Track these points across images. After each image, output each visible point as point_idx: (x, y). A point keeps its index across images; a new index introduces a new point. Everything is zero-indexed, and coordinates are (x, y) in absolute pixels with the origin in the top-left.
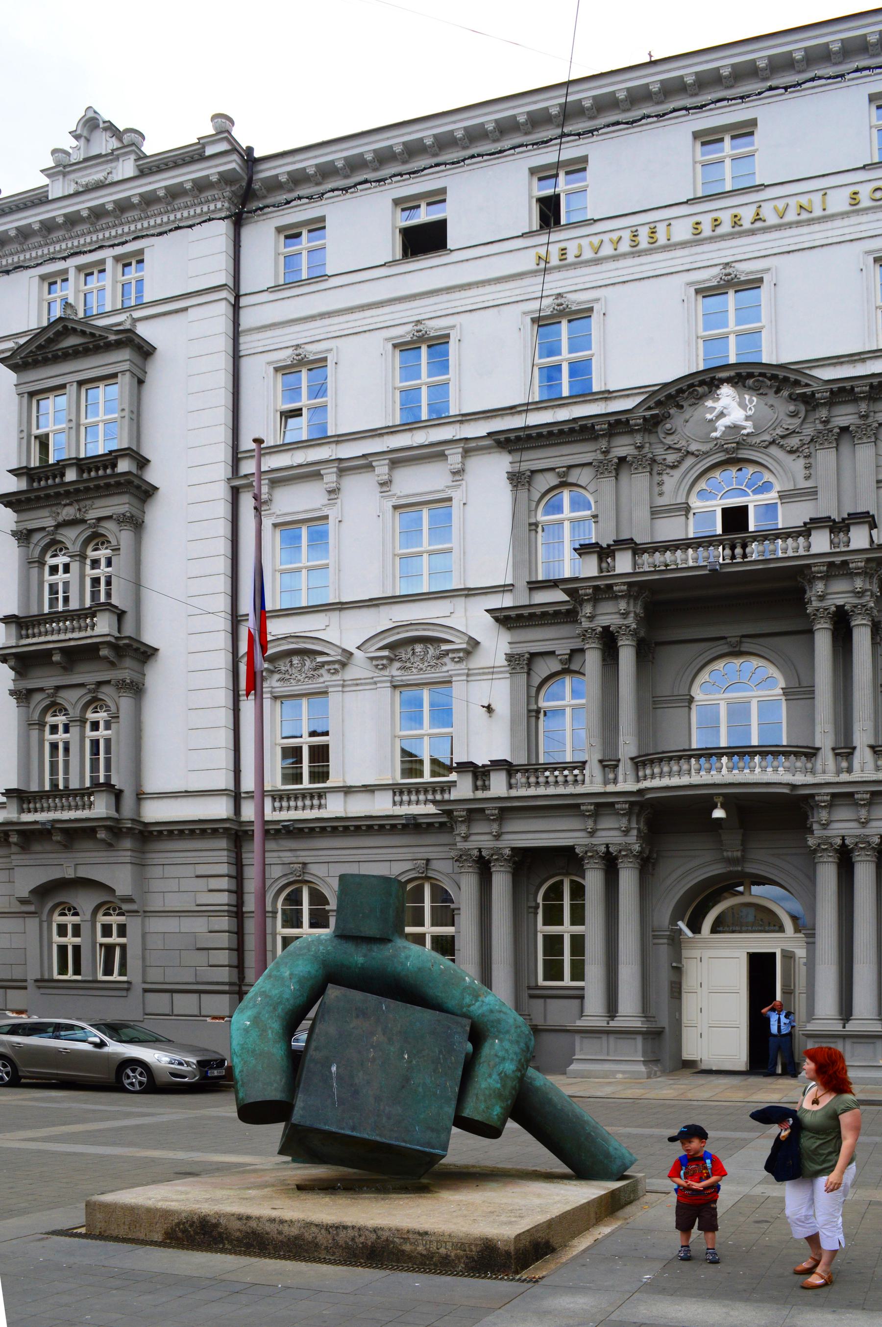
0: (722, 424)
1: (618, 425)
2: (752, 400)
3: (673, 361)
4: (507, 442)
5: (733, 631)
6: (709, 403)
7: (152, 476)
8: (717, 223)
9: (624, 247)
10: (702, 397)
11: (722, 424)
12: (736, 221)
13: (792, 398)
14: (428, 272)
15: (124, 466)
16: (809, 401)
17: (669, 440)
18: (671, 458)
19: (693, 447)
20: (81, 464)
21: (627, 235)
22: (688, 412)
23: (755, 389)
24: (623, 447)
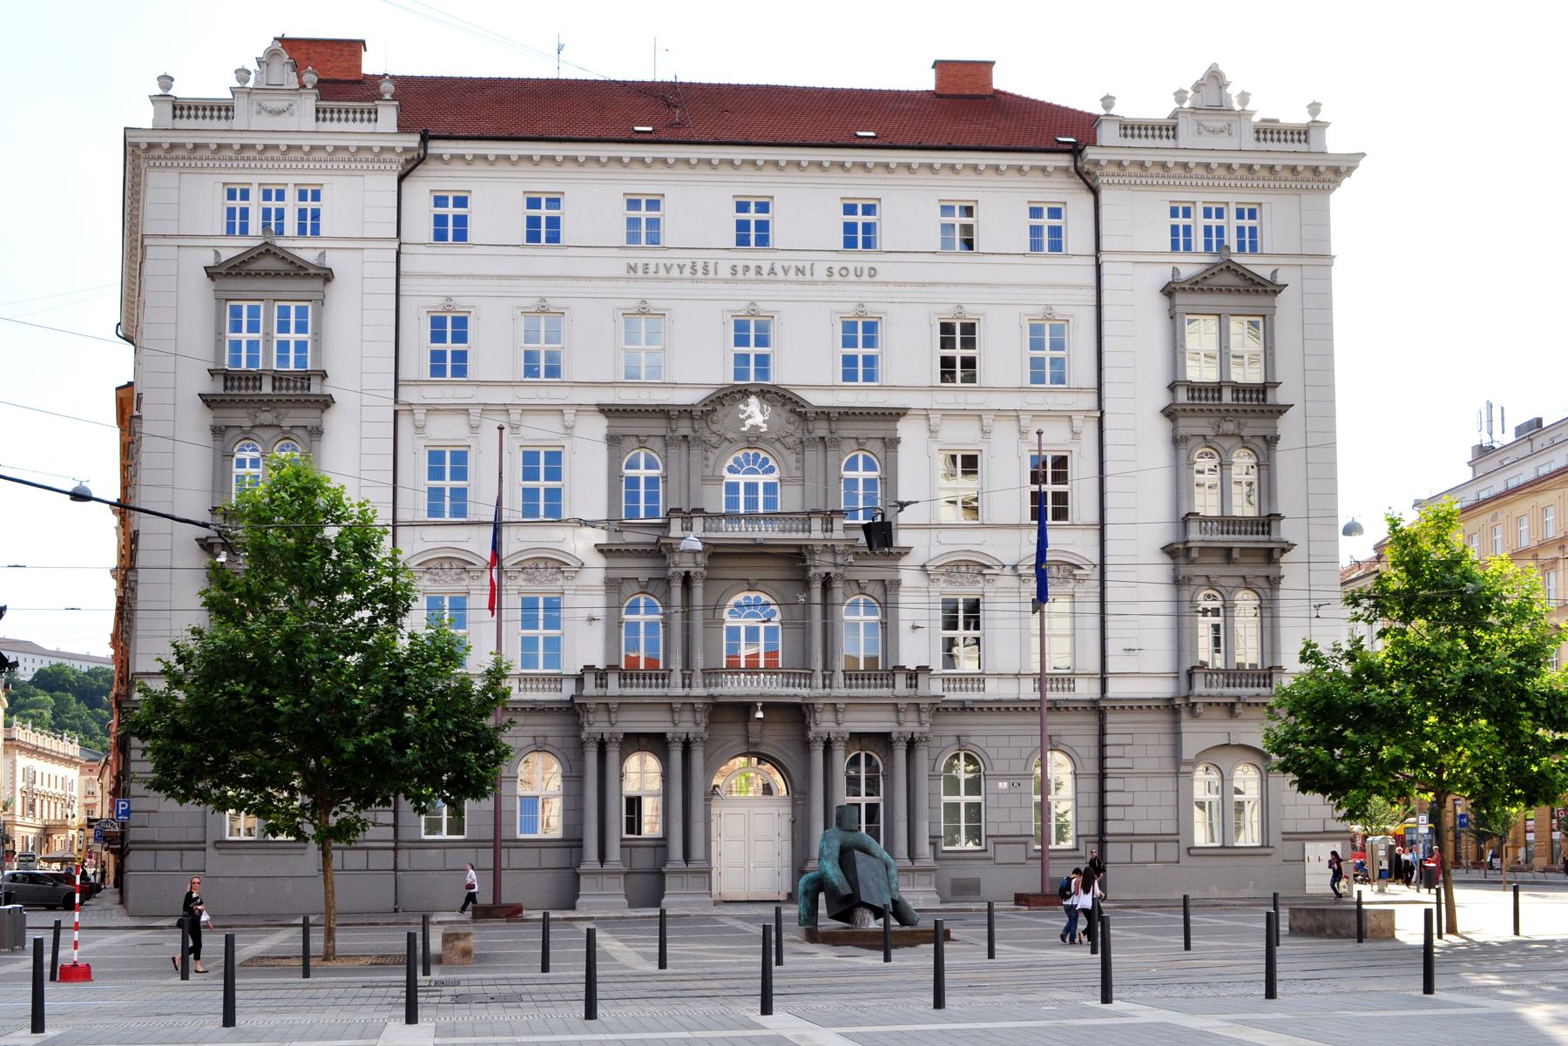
0: (749, 423)
1: (686, 412)
2: (768, 409)
3: (725, 376)
4: (606, 410)
5: (753, 575)
6: (741, 407)
7: (330, 388)
8: (747, 268)
9: (687, 272)
10: (735, 400)
11: (749, 423)
12: (759, 269)
13: (793, 411)
14: (544, 259)
15: (315, 388)
16: (803, 417)
17: (714, 427)
18: (714, 440)
19: (729, 436)
20: (277, 378)
21: (688, 263)
22: (727, 408)
23: (771, 402)
24: (684, 428)
